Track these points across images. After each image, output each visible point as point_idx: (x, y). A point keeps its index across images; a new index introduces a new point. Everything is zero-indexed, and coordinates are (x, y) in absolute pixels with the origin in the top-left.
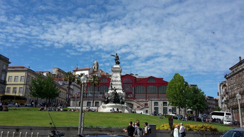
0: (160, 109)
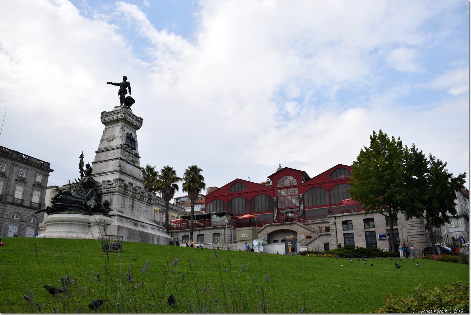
0: (358, 236)
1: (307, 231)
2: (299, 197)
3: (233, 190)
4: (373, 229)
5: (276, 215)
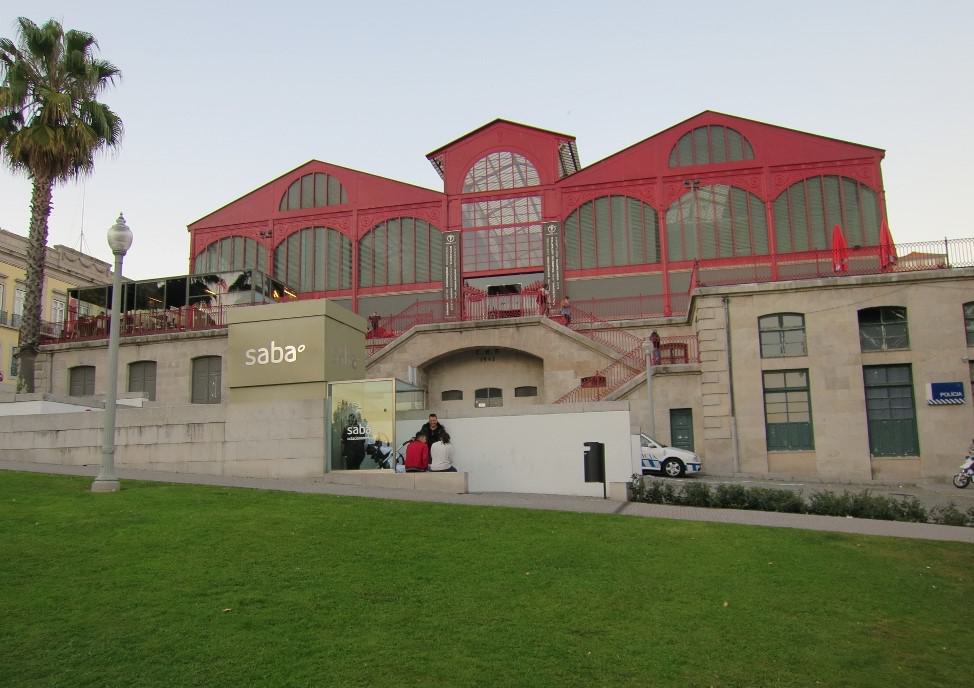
1: (585, 355)
2: (545, 231)
3: (294, 202)
4: (898, 357)
5: (453, 294)
